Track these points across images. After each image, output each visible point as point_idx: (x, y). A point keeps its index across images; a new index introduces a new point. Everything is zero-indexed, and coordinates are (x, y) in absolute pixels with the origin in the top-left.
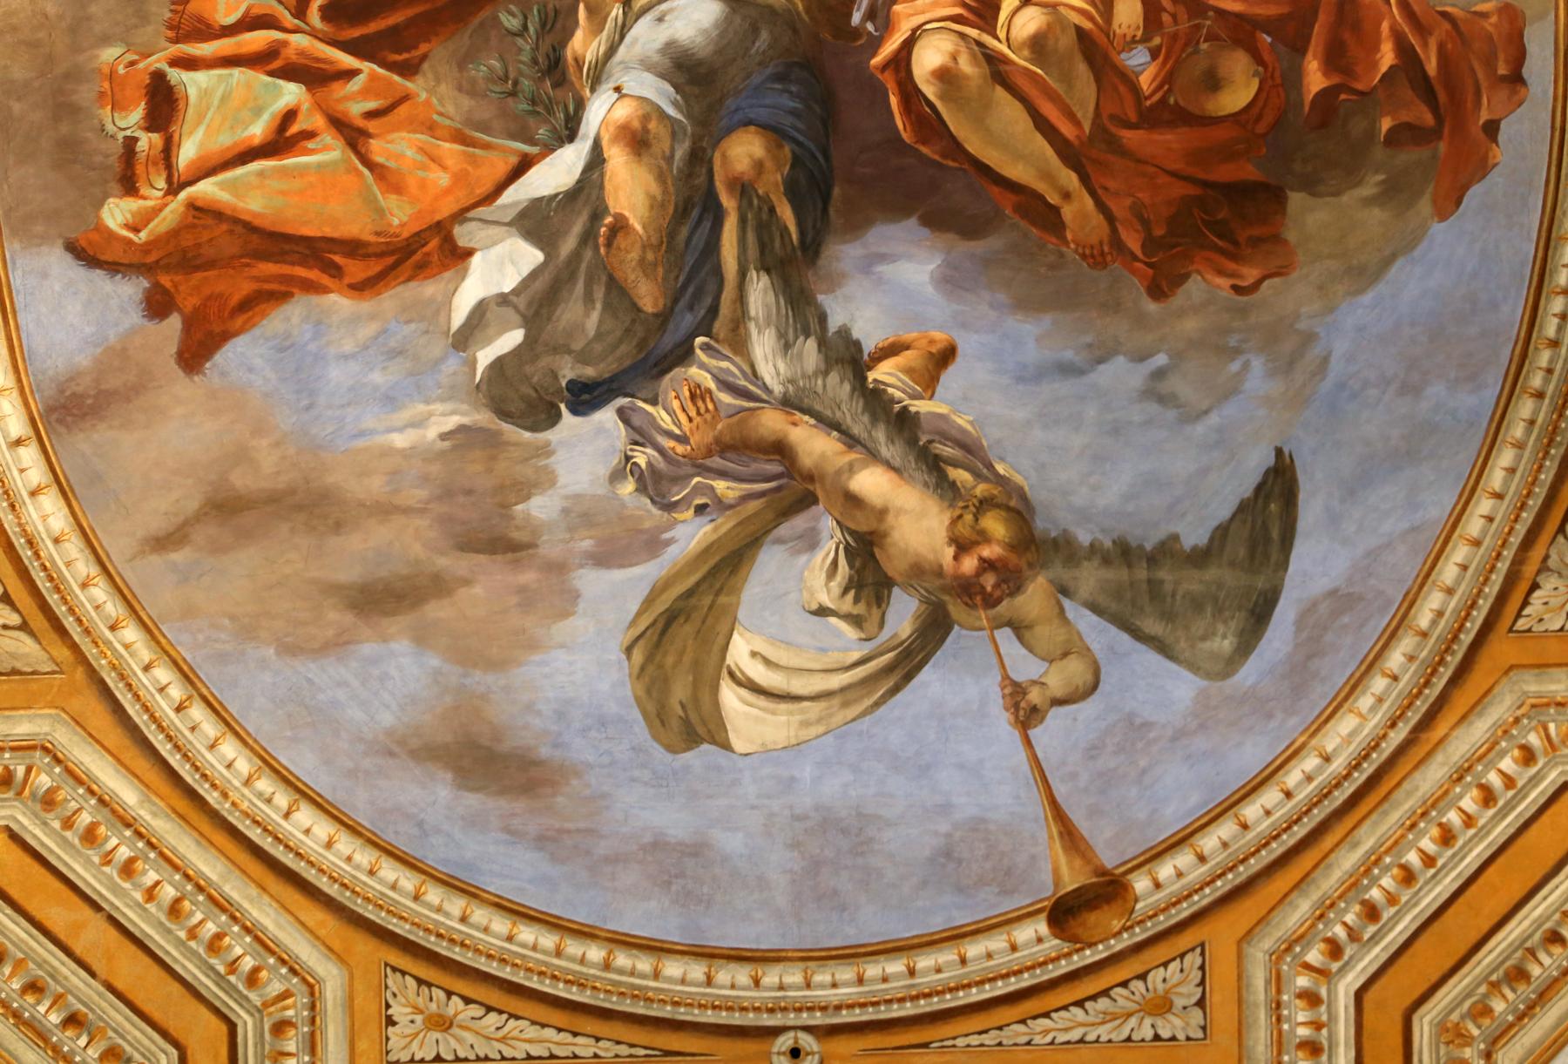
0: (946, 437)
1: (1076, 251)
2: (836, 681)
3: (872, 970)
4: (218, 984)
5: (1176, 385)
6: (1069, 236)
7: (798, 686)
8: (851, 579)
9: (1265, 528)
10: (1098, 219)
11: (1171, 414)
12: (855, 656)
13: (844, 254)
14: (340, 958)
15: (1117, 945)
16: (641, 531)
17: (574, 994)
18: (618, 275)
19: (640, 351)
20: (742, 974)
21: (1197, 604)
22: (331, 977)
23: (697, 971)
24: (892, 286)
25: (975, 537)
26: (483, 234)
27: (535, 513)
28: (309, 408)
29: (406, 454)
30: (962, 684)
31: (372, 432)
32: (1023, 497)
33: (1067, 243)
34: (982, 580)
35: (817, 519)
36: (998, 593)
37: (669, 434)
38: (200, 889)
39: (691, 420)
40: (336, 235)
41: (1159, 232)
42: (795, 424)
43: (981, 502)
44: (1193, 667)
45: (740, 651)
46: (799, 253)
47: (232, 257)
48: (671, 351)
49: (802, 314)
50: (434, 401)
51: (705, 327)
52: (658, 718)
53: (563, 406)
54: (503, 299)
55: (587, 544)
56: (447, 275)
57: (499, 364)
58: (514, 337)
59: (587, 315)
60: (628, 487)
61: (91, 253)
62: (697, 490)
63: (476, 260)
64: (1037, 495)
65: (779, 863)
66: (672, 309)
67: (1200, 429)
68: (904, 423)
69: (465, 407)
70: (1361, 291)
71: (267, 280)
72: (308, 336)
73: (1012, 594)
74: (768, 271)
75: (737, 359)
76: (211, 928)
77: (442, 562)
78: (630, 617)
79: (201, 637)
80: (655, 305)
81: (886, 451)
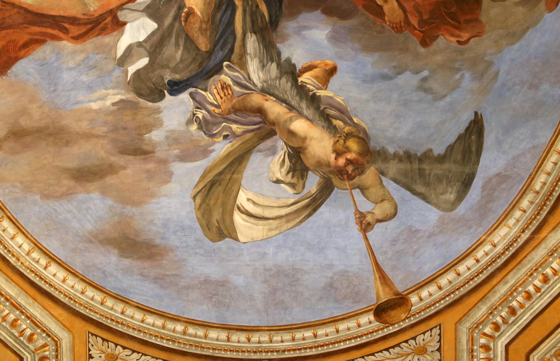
0: (332, 107)
1: (389, 25)
2: (284, 211)
3: (299, 335)
4: (15, 341)
5: (431, 84)
6: (387, 19)
7: (267, 213)
8: (290, 167)
9: (469, 145)
10: (399, 12)
11: (430, 97)
12: (292, 201)
13: (288, 26)
14: (69, 330)
15: (403, 325)
16: (200, 146)
17: (170, 345)
18: (190, 34)
19: (199, 68)
20: (243, 337)
21: (439, 179)
22: (65, 337)
23: (223, 335)
25: (344, 150)
26: (131, 15)
27: (153, 138)
28: (55, 90)
29: (97, 112)
30: (337, 213)
31: (82, 102)
32: (365, 132)
33: (386, 23)
34: (347, 168)
35: (276, 141)
36: (354, 174)
37: (212, 104)
38: (7, 300)
39: (221, 98)
40: (66, 15)
41: (426, 17)
42: (267, 100)
43: (347, 135)
44: (437, 206)
45: (242, 199)
46: (269, 25)
47: (20, 24)
48: (213, 68)
49: (270, 52)
50: (110, 89)
51: (228, 58)
52: (207, 227)
53: (166, 92)
54: (139, 44)
55: (176, 152)
56: (115, 33)
57: (138, 73)
58: (144, 61)
59: (176, 52)
60: (194, 127)
62: (224, 128)
63: (128, 26)
64: (371, 132)
65: (259, 289)
66: (214, 49)
67: (442, 103)
68: (314, 100)
69: (123, 91)
70: (513, 44)
71: (35, 34)
72: (54, 59)
73: (360, 174)
74: (255, 33)
75: (242, 72)
76: (12, 317)
77: (113, 159)
78: (195, 184)
79: (7, 191)
80: (206, 48)
81: (306, 112)
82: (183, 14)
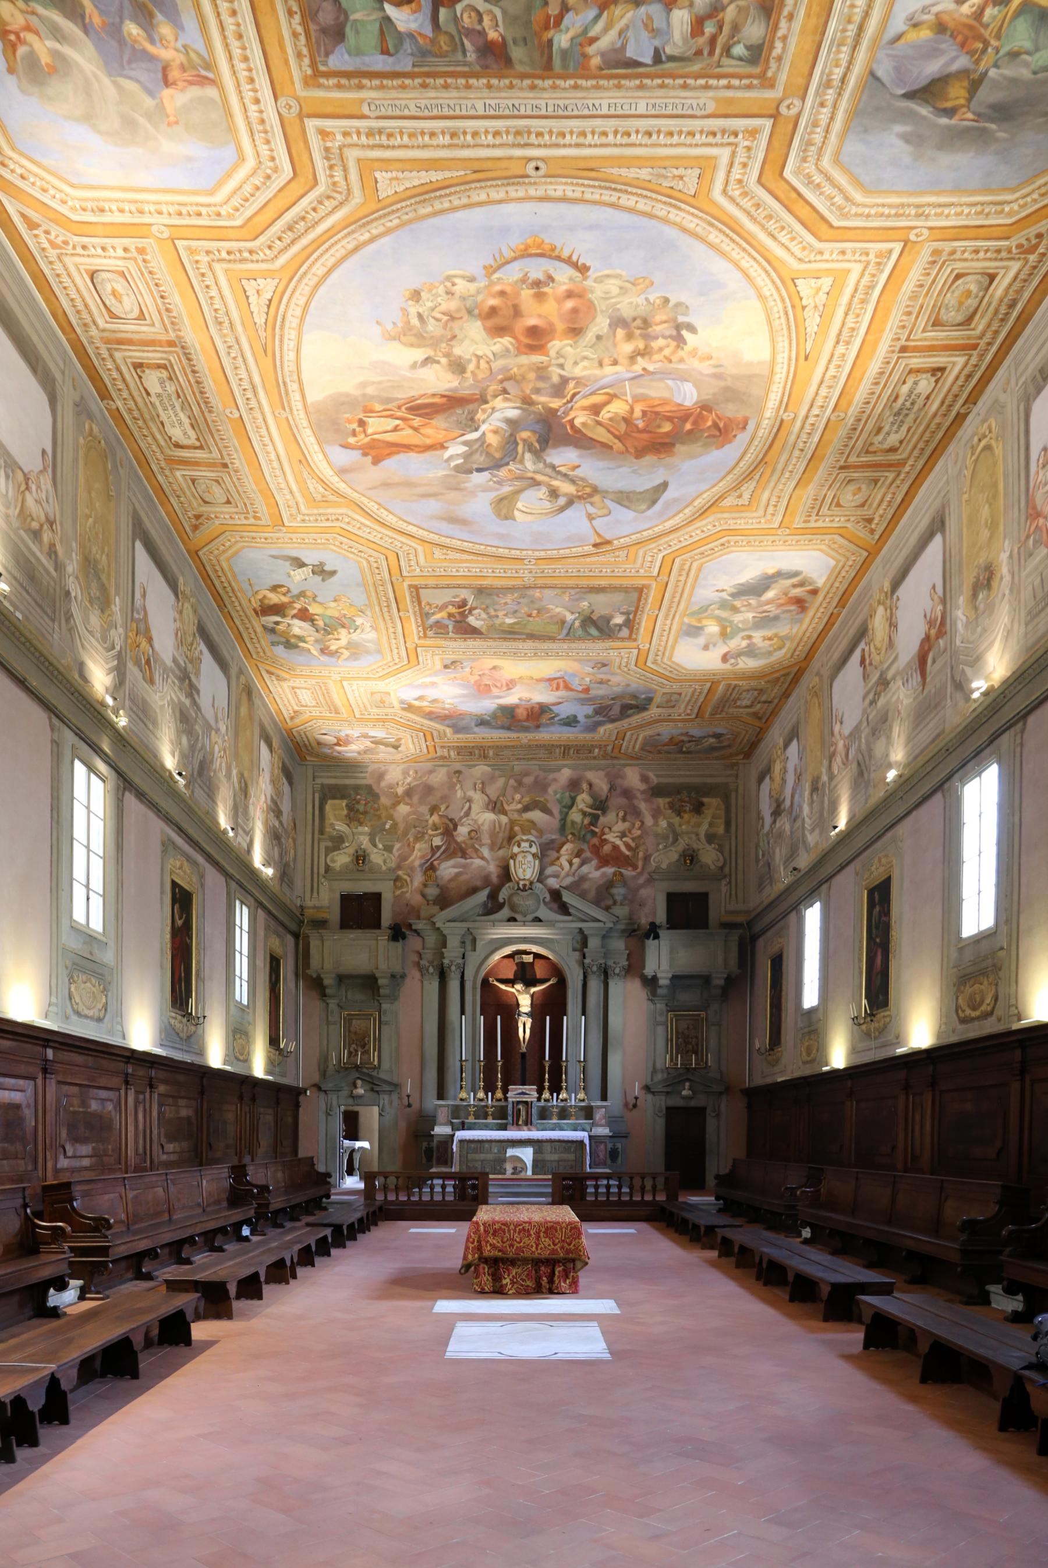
22: (420, 549)
24: (563, 457)
45: (519, 505)
52: (498, 515)
57: (457, 466)
61: (346, 446)
82: (522, 1019)
